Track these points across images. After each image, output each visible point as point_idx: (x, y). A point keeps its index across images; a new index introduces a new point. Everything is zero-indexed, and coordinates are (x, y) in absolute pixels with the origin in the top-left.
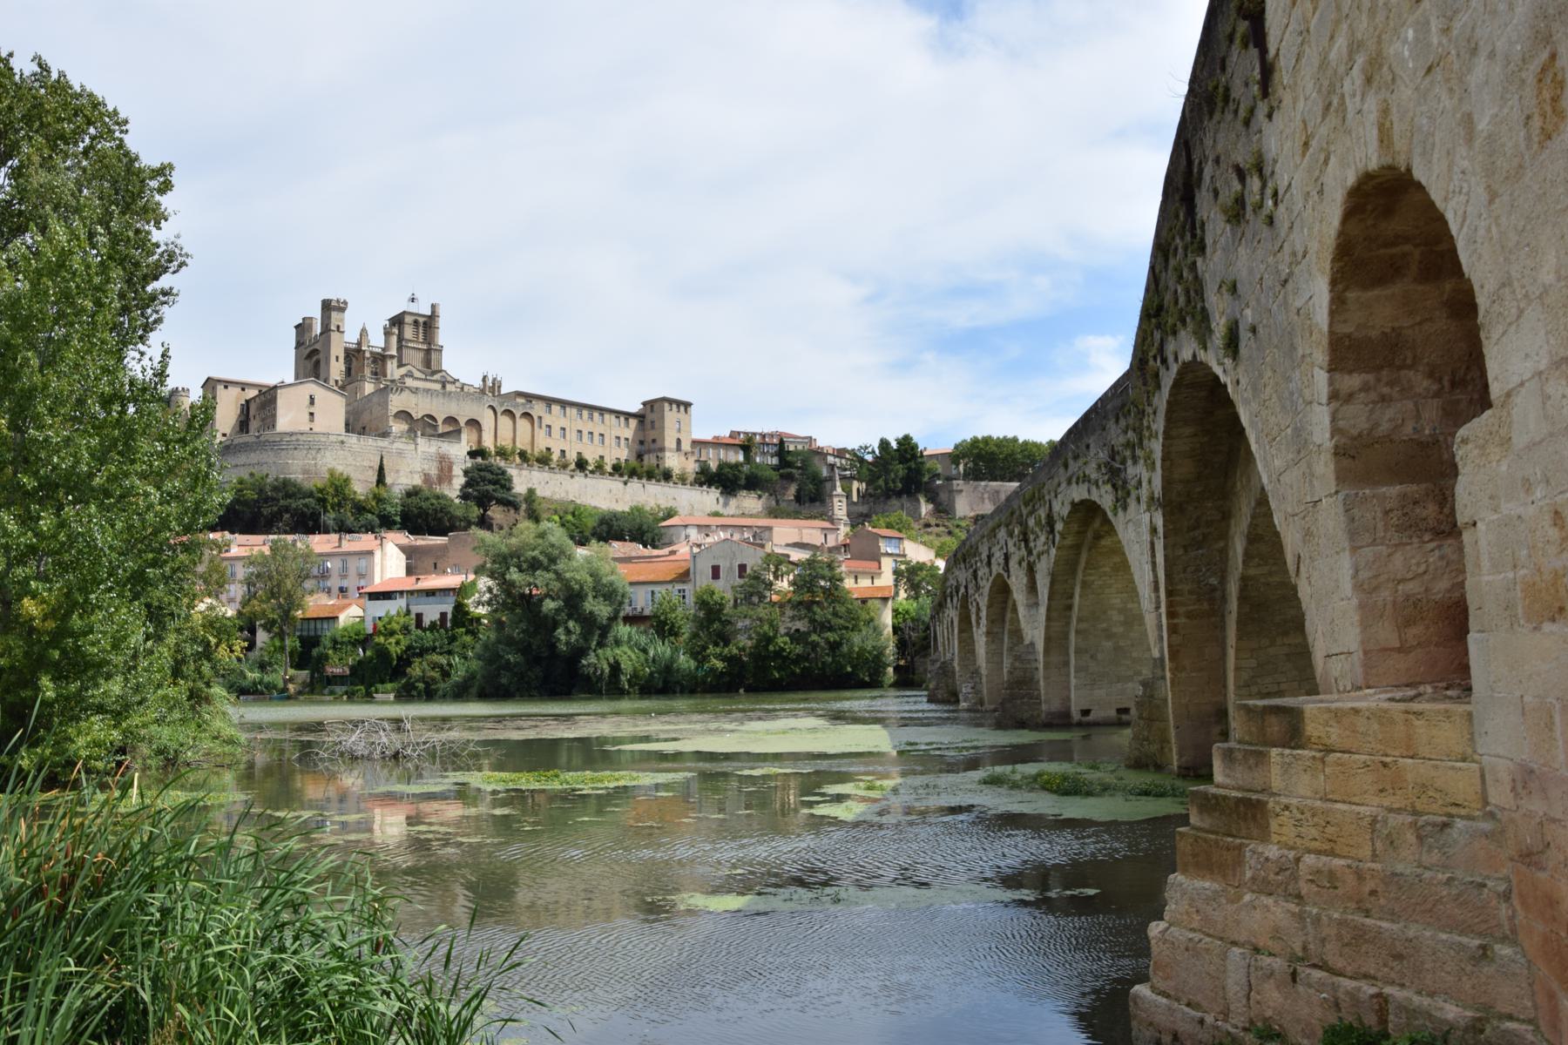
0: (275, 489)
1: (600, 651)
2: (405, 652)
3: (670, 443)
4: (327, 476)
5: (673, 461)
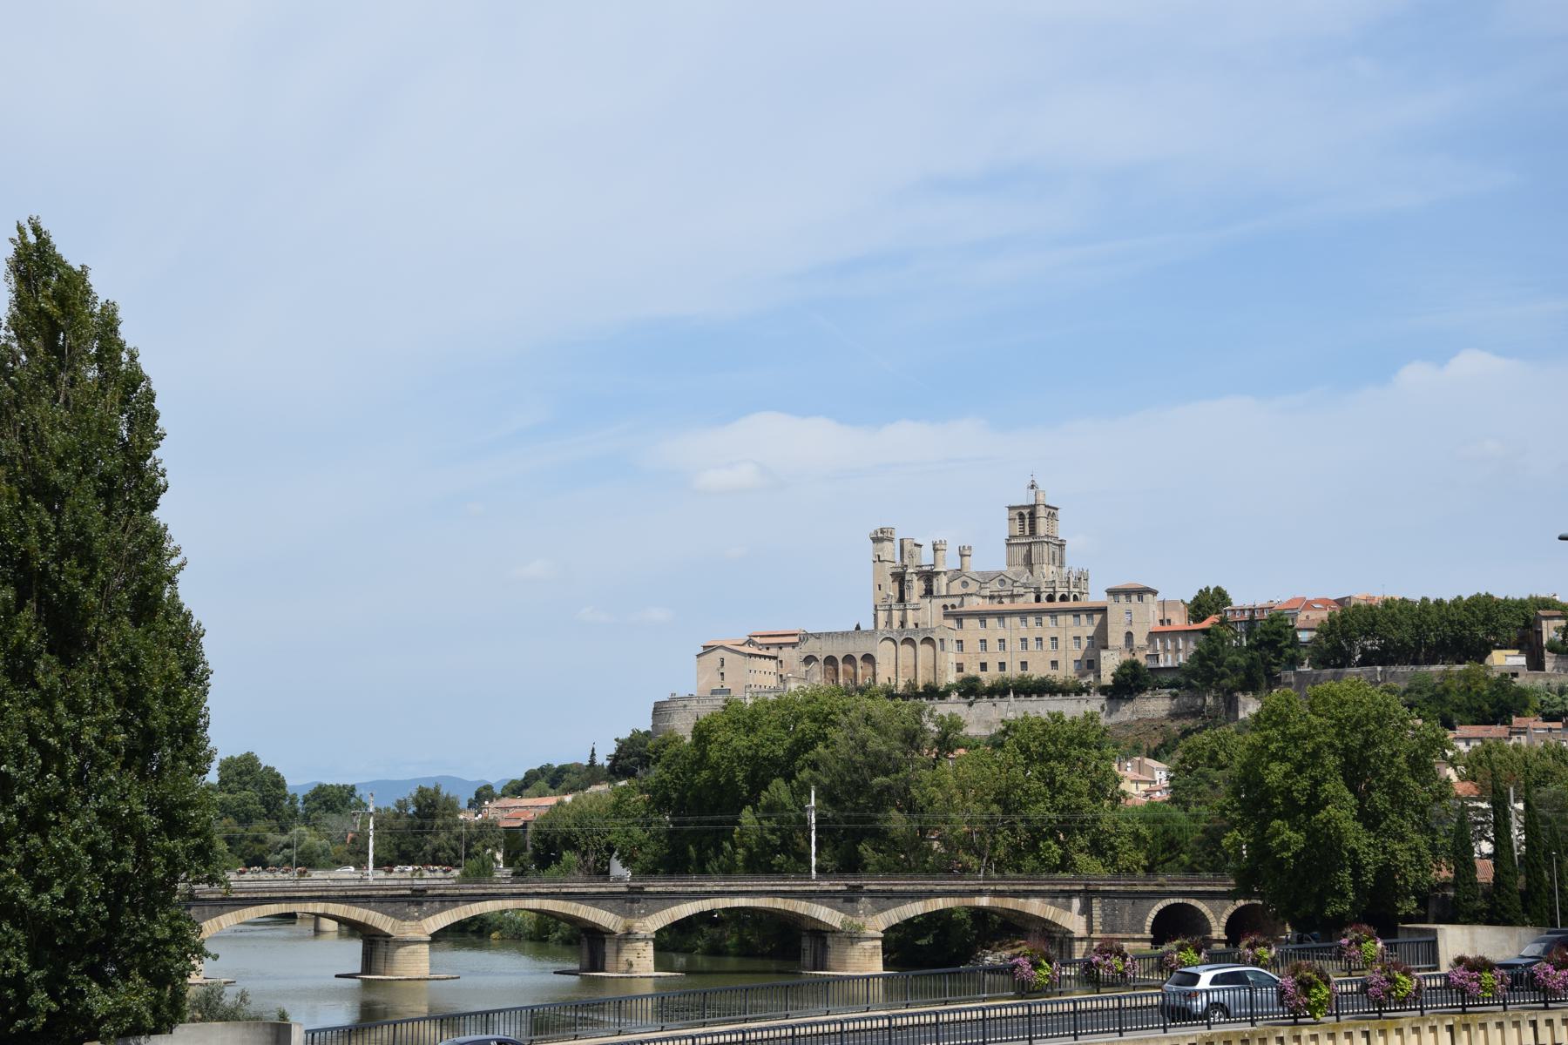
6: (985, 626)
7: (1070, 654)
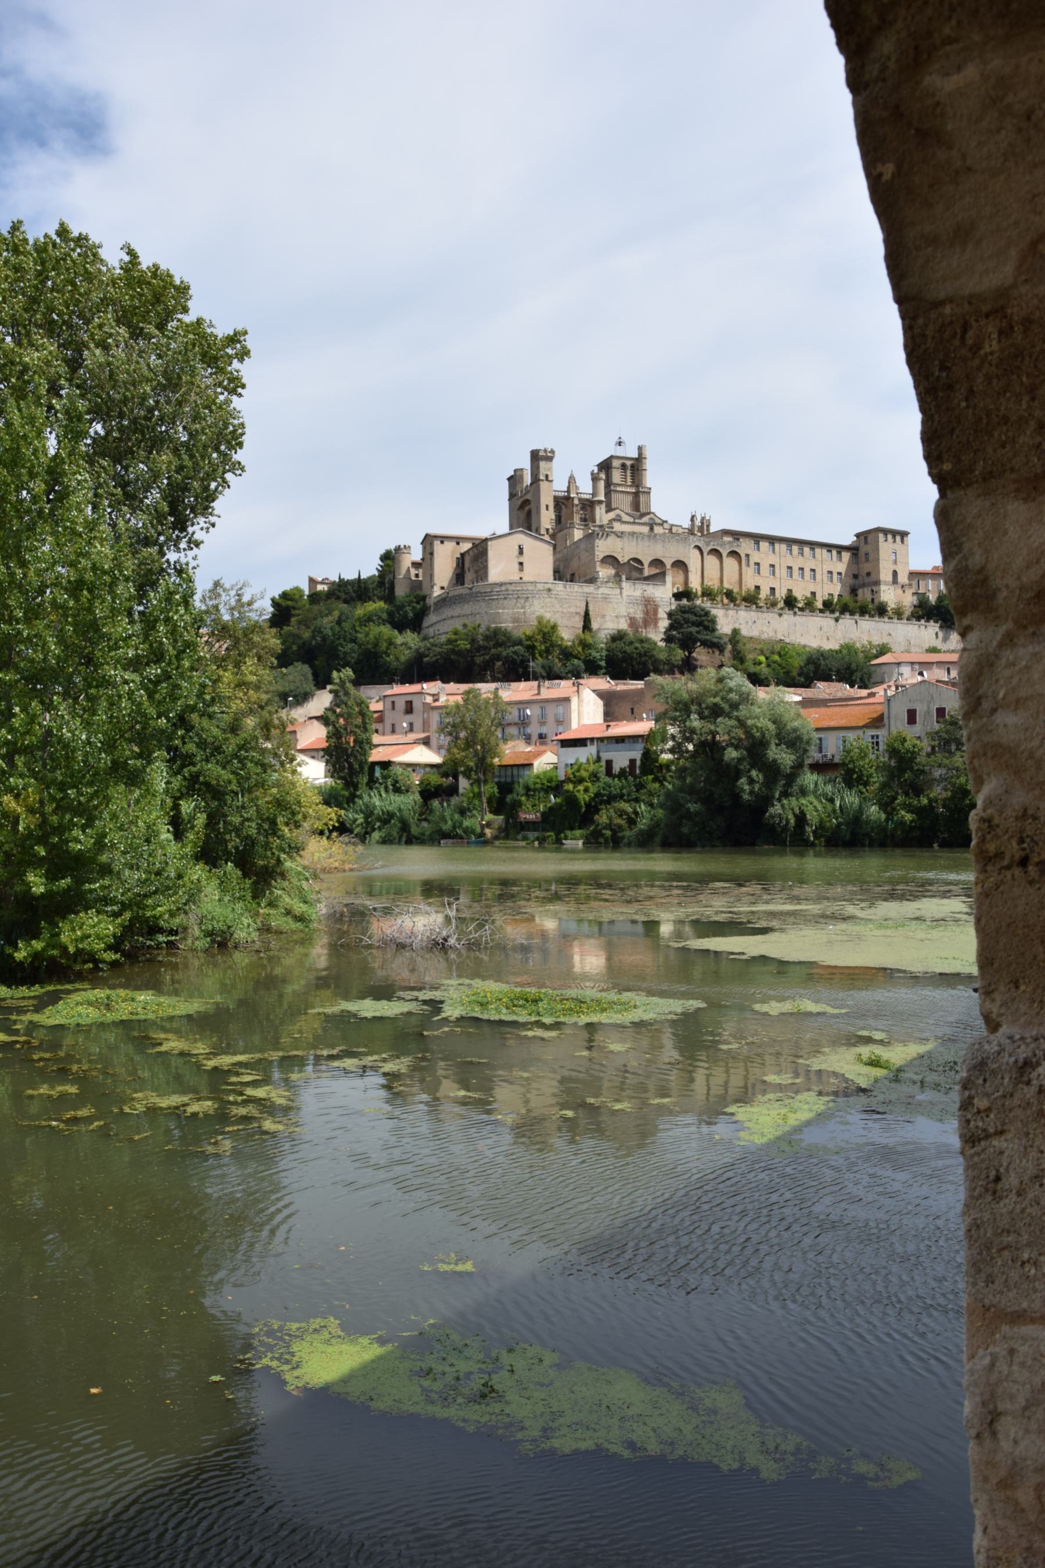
0: (487, 638)
1: (785, 801)
2: (593, 799)
3: (885, 575)
4: (535, 623)
5: (888, 595)
6: (758, 549)
7: (825, 586)
